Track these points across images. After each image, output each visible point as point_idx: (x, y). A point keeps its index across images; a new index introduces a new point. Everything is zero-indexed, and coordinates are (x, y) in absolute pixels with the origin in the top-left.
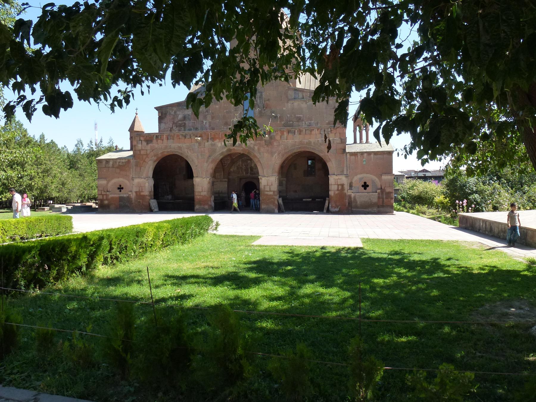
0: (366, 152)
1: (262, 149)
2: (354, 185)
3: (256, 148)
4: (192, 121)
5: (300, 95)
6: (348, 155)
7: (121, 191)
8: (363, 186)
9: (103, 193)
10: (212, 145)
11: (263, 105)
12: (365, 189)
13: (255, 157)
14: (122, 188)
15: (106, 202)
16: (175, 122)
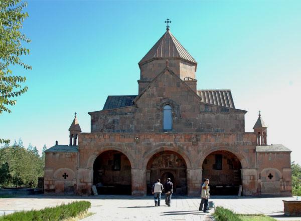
0: (271, 152)
1: (190, 148)
2: (262, 176)
3: (185, 147)
4: (120, 125)
5: (210, 110)
6: (258, 154)
7: (65, 178)
8: (269, 177)
9: (49, 180)
10: (148, 144)
11: (180, 115)
12: (270, 178)
13: (184, 154)
14: (67, 176)
15: (52, 187)
16: (107, 123)
